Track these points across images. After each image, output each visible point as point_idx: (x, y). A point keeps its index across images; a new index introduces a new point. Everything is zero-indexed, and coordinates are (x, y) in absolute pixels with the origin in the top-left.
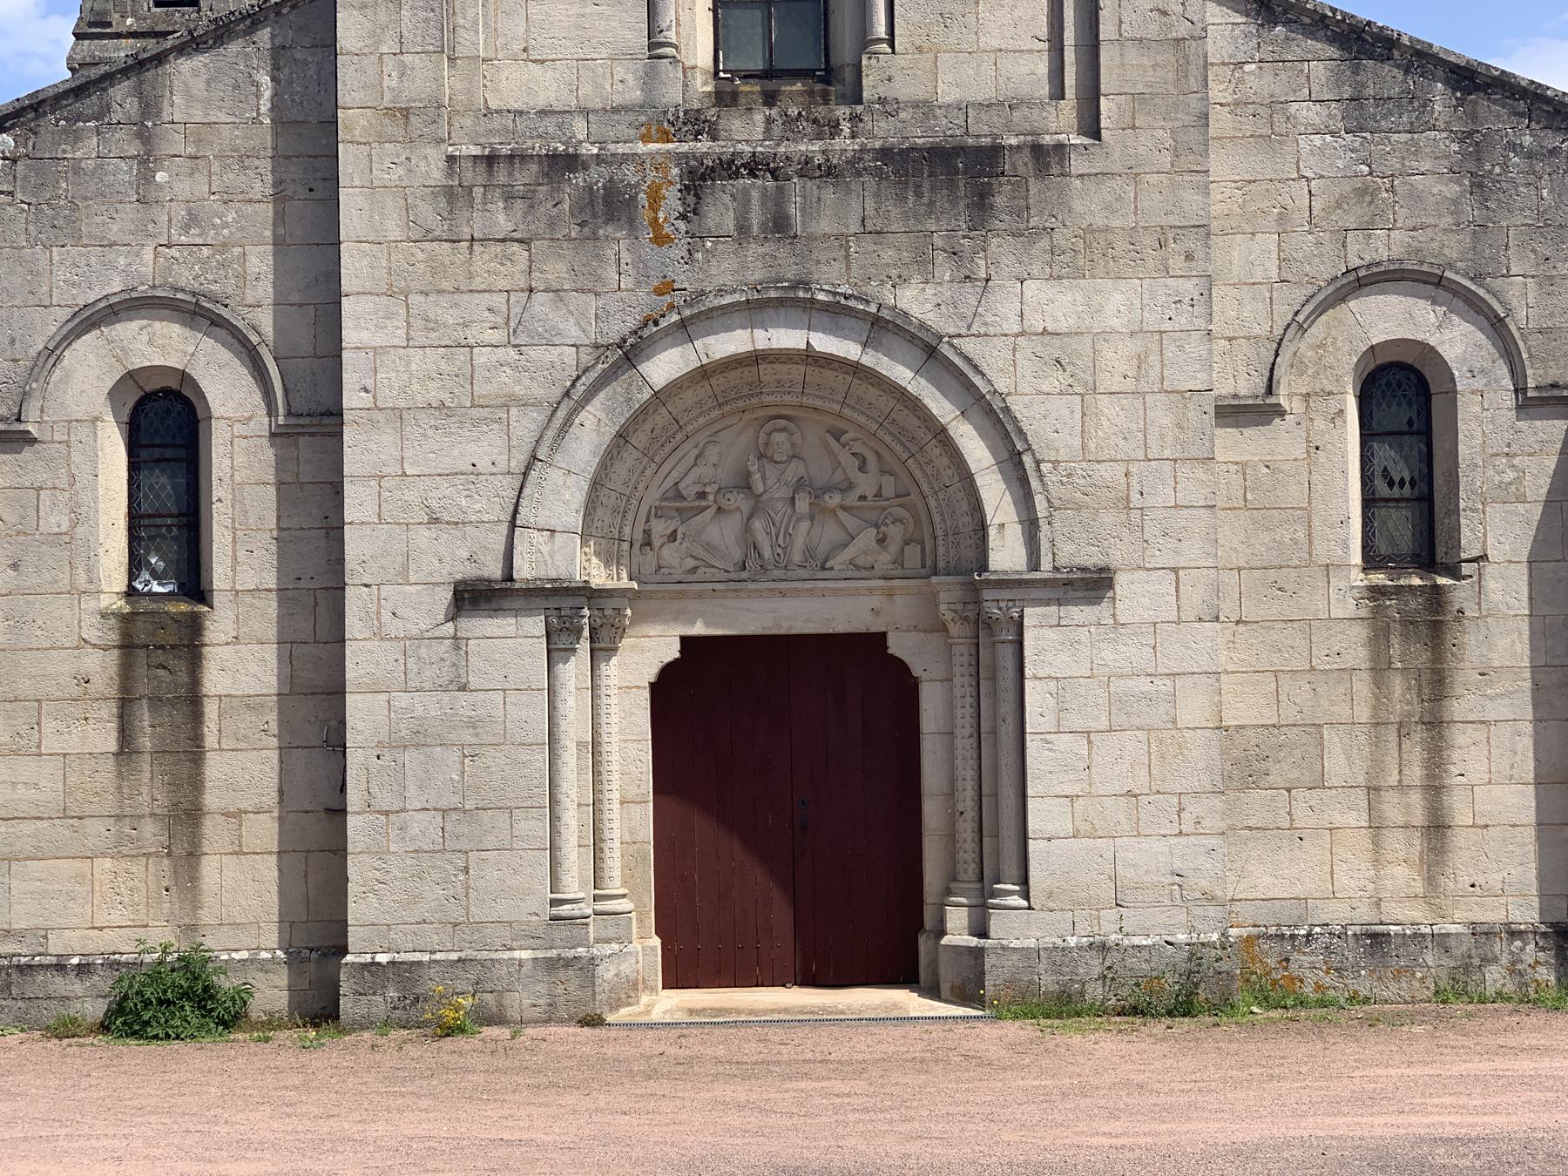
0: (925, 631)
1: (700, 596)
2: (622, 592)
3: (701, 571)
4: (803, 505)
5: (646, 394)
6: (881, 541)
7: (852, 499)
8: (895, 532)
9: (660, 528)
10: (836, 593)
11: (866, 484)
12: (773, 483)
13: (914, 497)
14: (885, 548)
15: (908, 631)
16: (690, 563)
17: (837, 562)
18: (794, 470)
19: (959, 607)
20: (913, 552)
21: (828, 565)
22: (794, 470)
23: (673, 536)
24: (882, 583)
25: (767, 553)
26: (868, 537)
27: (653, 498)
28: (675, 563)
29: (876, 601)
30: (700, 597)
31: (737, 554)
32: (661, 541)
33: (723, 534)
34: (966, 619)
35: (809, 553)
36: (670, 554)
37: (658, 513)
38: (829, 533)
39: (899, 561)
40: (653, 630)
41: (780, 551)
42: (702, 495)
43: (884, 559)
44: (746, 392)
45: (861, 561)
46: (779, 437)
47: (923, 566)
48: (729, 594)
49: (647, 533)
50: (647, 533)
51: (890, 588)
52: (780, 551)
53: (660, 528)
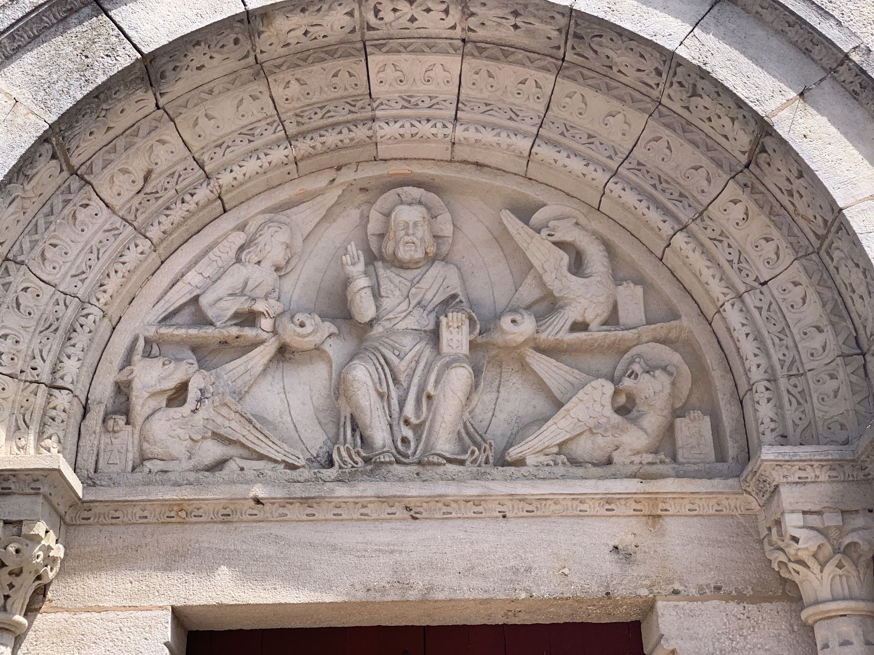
0: (740, 598)
1: (226, 517)
2: (38, 482)
3: (232, 465)
4: (456, 337)
5: (126, 58)
6: (626, 408)
7: (557, 330)
8: (652, 389)
9: (151, 377)
10: (533, 508)
11: (585, 298)
12: (396, 305)
13: (689, 322)
14: (634, 421)
15: (702, 596)
16: (212, 451)
17: (527, 449)
18: (436, 282)
19: (832, 520)
20: (694, 433)
21: (514, 453)
22: (436, 282)
23: (178, 395)
24: (633, 486)
25: (380, 435)
26: (594, 401)
27: (142, 320)
28: (179, 449)
29: (623, 530)
30: (226, 518)
31: (316, 439)
32: (153, 404)
33: (292, 402)
34: (848, 551)
35: (471, 438)
36: (168, 430)
37: (152, 348)
38: (512, 399)
39: (666, 444)
40: (106, 587)
41: (408, 433)
42: (248, 318)
43: (635, 440)
44: (342, 115)
45: (584, 448)
46: (408, 214)
47: (721, 457)
48: (295, 512)
49: (122, 390)
50: (122, 390)
51: (654, 498)
52: (408, 433)
53: (151, 377)
